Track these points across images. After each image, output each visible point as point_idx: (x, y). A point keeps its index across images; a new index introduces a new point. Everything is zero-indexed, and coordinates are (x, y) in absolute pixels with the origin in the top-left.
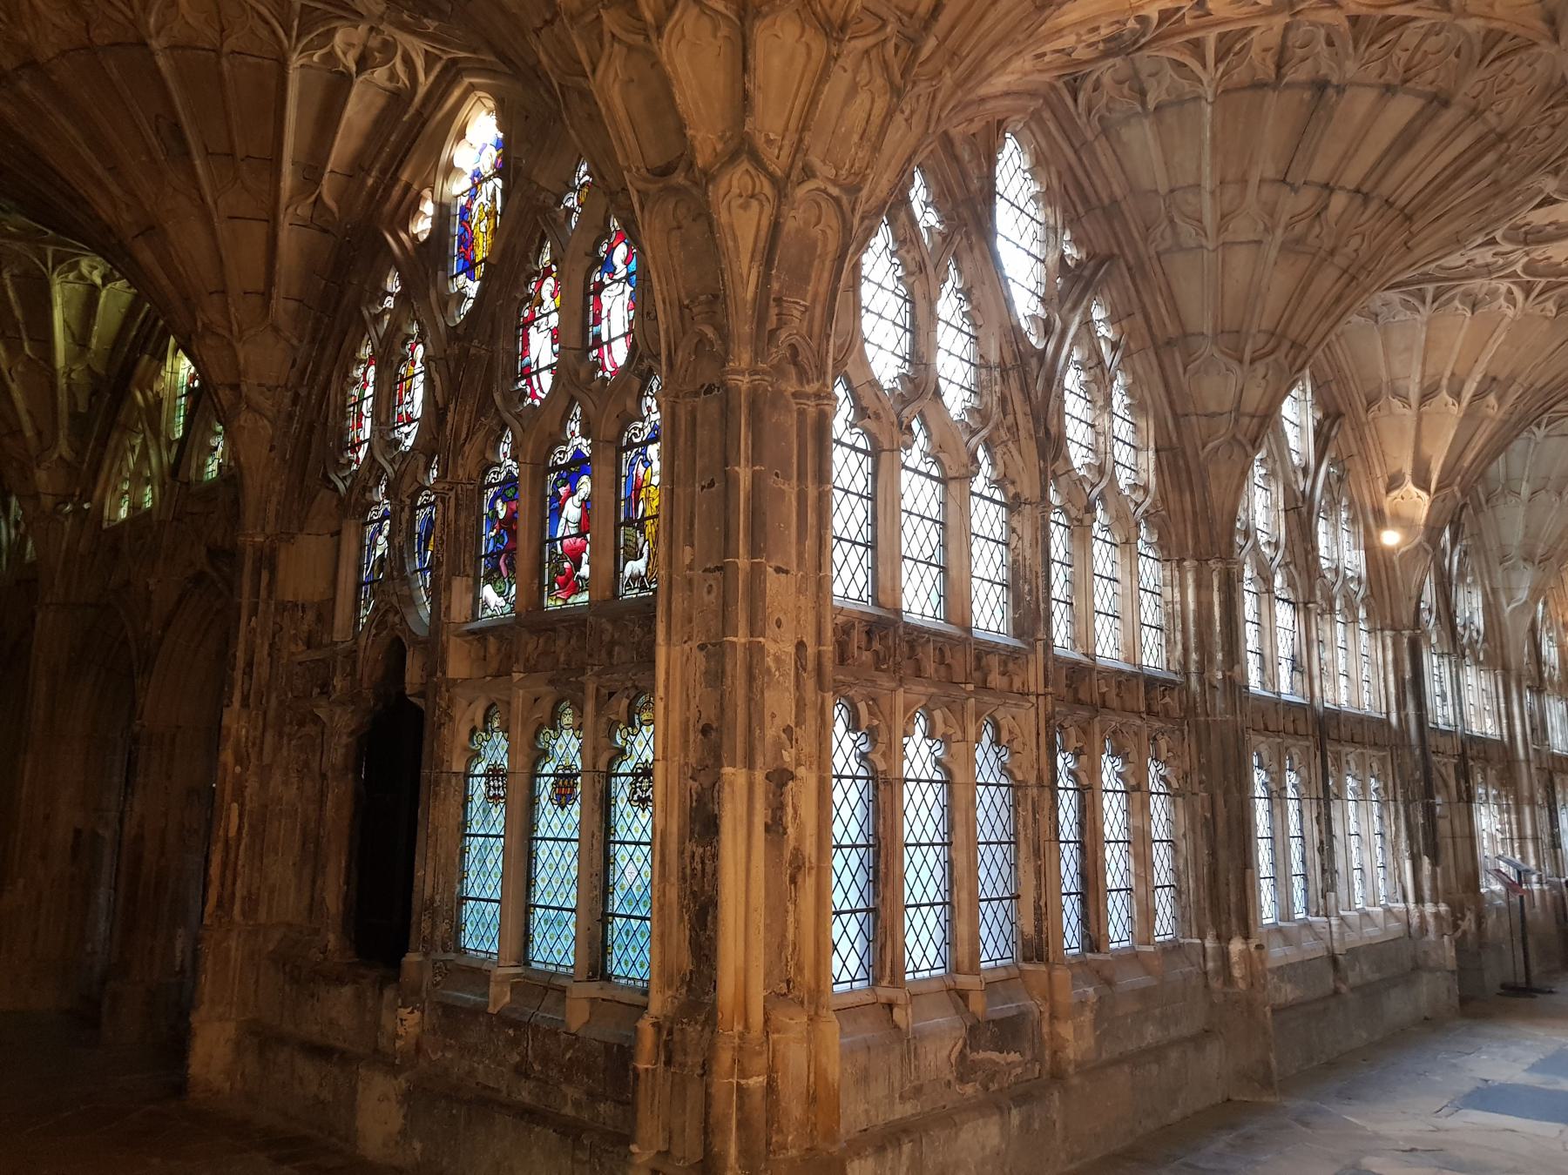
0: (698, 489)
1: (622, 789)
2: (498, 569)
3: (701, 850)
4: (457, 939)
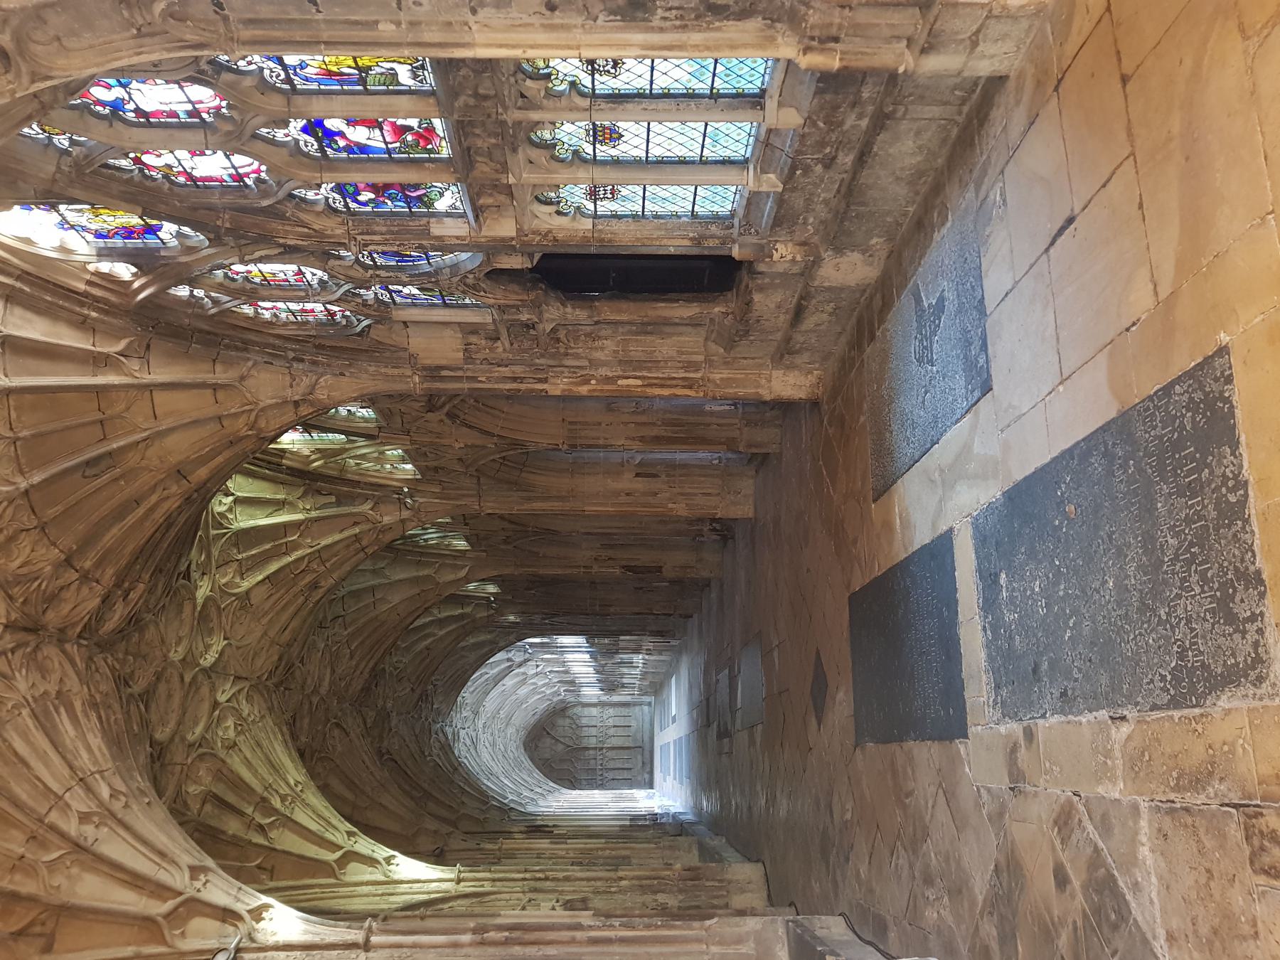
0: (320, 16)
1: (605, 84)
2: (419, 198)
3: (659, 11)
4: (724, 218)
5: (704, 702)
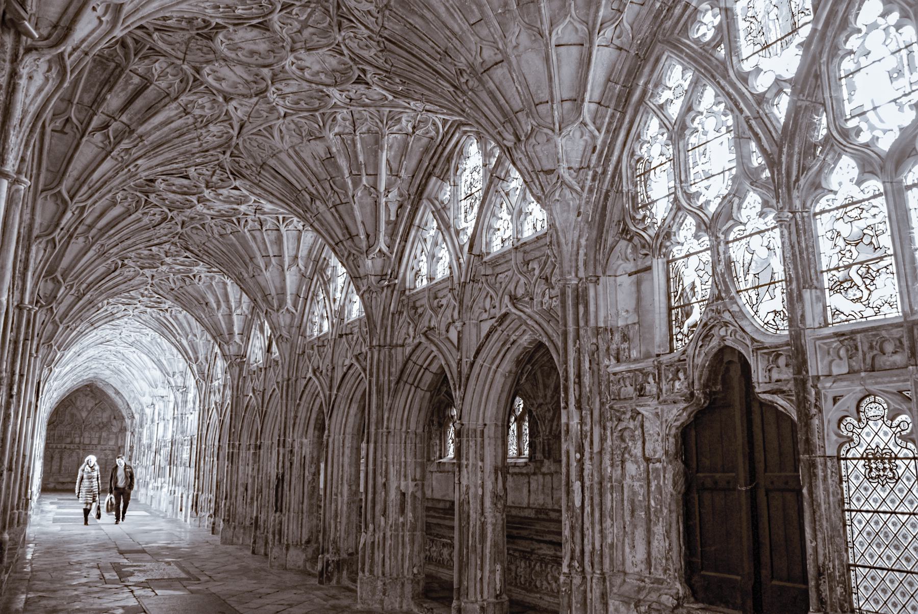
5: (139, 547)
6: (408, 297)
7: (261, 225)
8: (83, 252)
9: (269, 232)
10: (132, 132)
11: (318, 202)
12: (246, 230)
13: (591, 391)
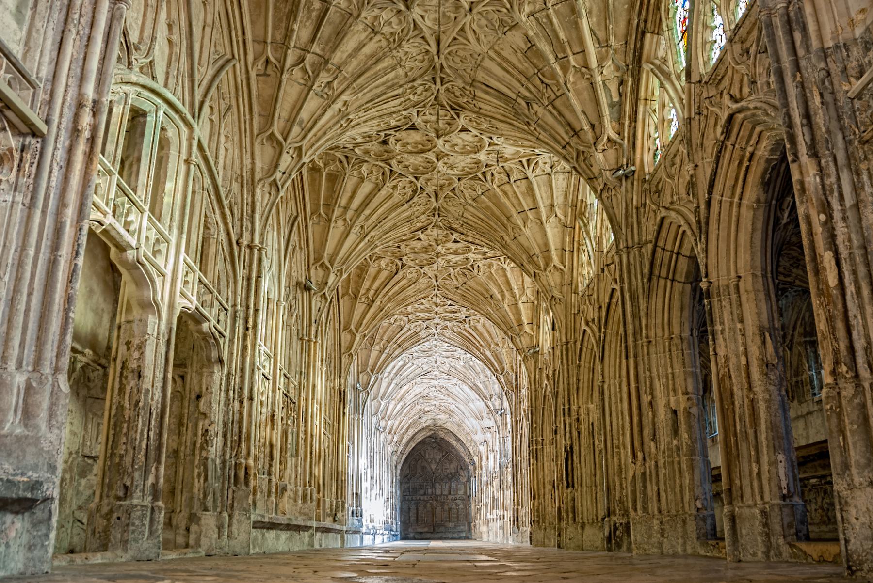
6: (650, 182)
7: (509, 176)
8: (345, 235)
9: (518, 182)
10: (327, 62)
11: (535, 106)
12: (495, 186)
13: (828, 131)
